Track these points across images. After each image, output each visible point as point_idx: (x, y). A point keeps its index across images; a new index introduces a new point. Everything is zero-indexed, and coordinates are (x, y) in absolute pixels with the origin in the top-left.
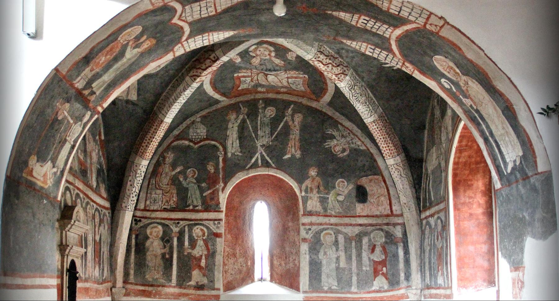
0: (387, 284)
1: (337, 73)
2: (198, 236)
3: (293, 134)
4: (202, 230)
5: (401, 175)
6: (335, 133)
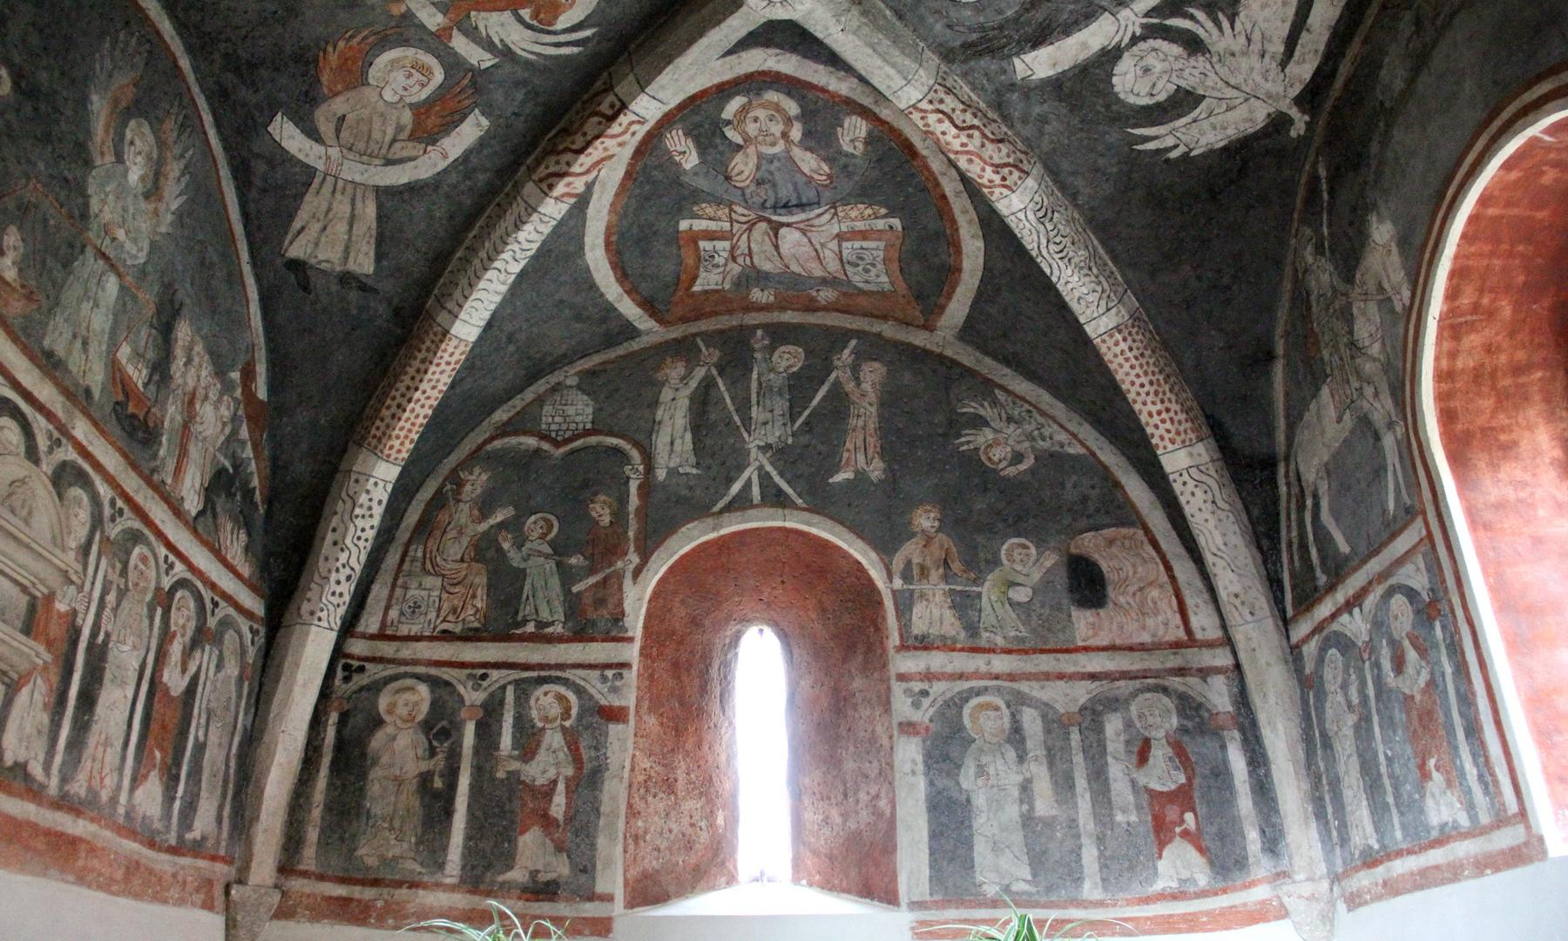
0: (1207, 870)
1: (996, 160)
2: (546, 719)
3: (858, 416)
4: (560, 698)
5: (1213, 502)
6: (987, 412)
